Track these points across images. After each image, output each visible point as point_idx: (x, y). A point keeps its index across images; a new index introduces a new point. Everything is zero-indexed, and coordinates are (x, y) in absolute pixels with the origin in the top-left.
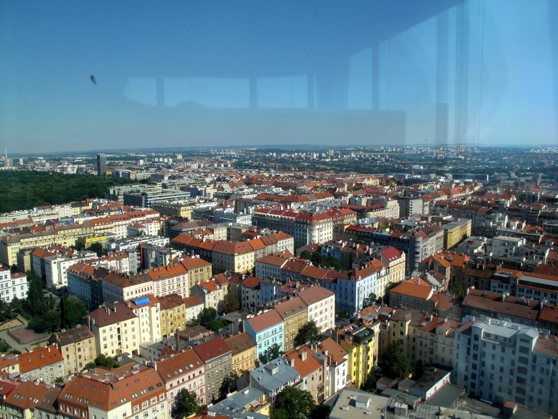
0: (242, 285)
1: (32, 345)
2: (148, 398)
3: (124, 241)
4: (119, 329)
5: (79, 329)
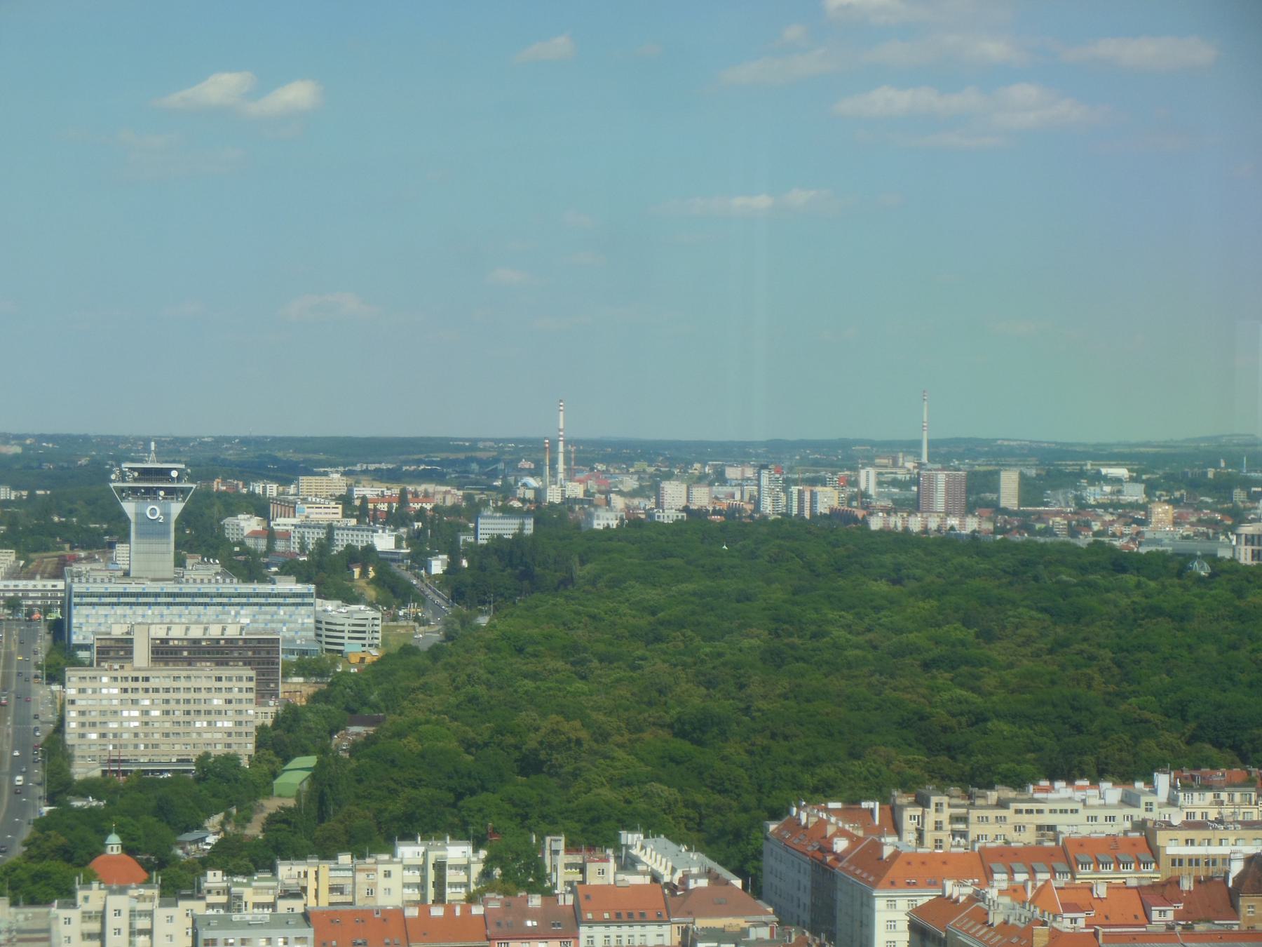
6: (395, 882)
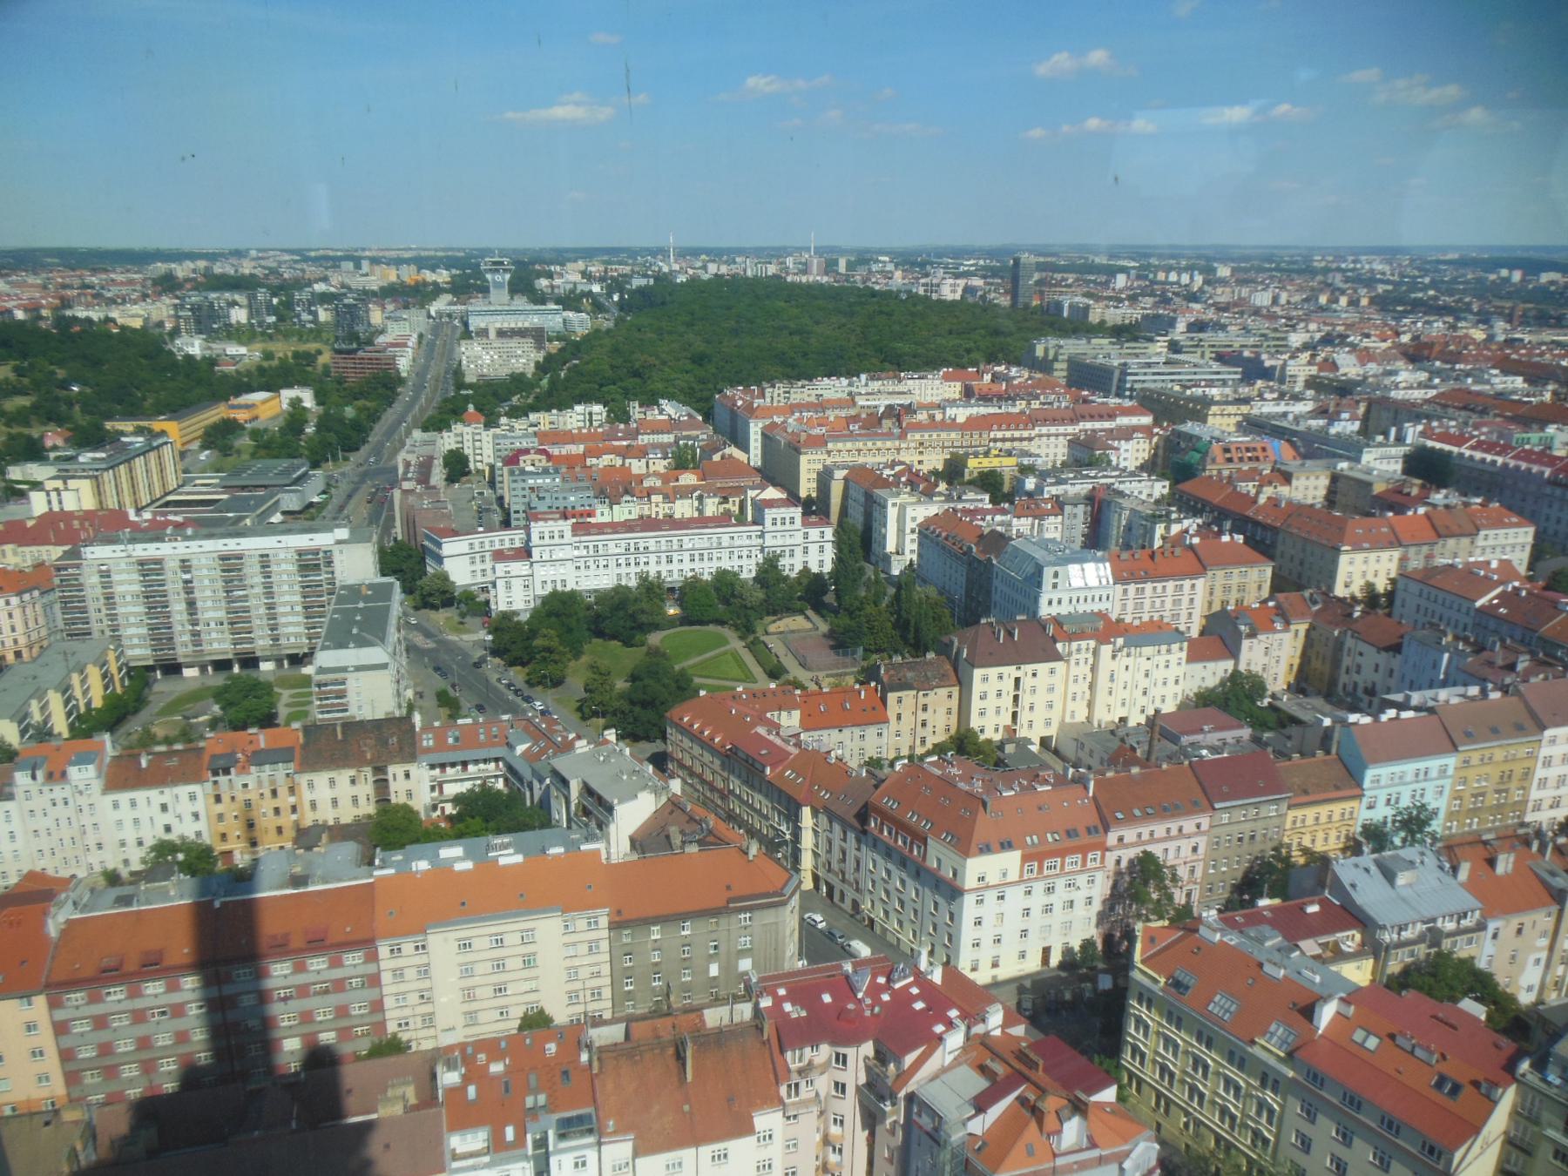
0: (1349, 633)
1: (828, 676)
2: (1062, 853)
3: (1054, 474)
4: (1017, 680)
5: (931, 663)
6: (574, 420)
